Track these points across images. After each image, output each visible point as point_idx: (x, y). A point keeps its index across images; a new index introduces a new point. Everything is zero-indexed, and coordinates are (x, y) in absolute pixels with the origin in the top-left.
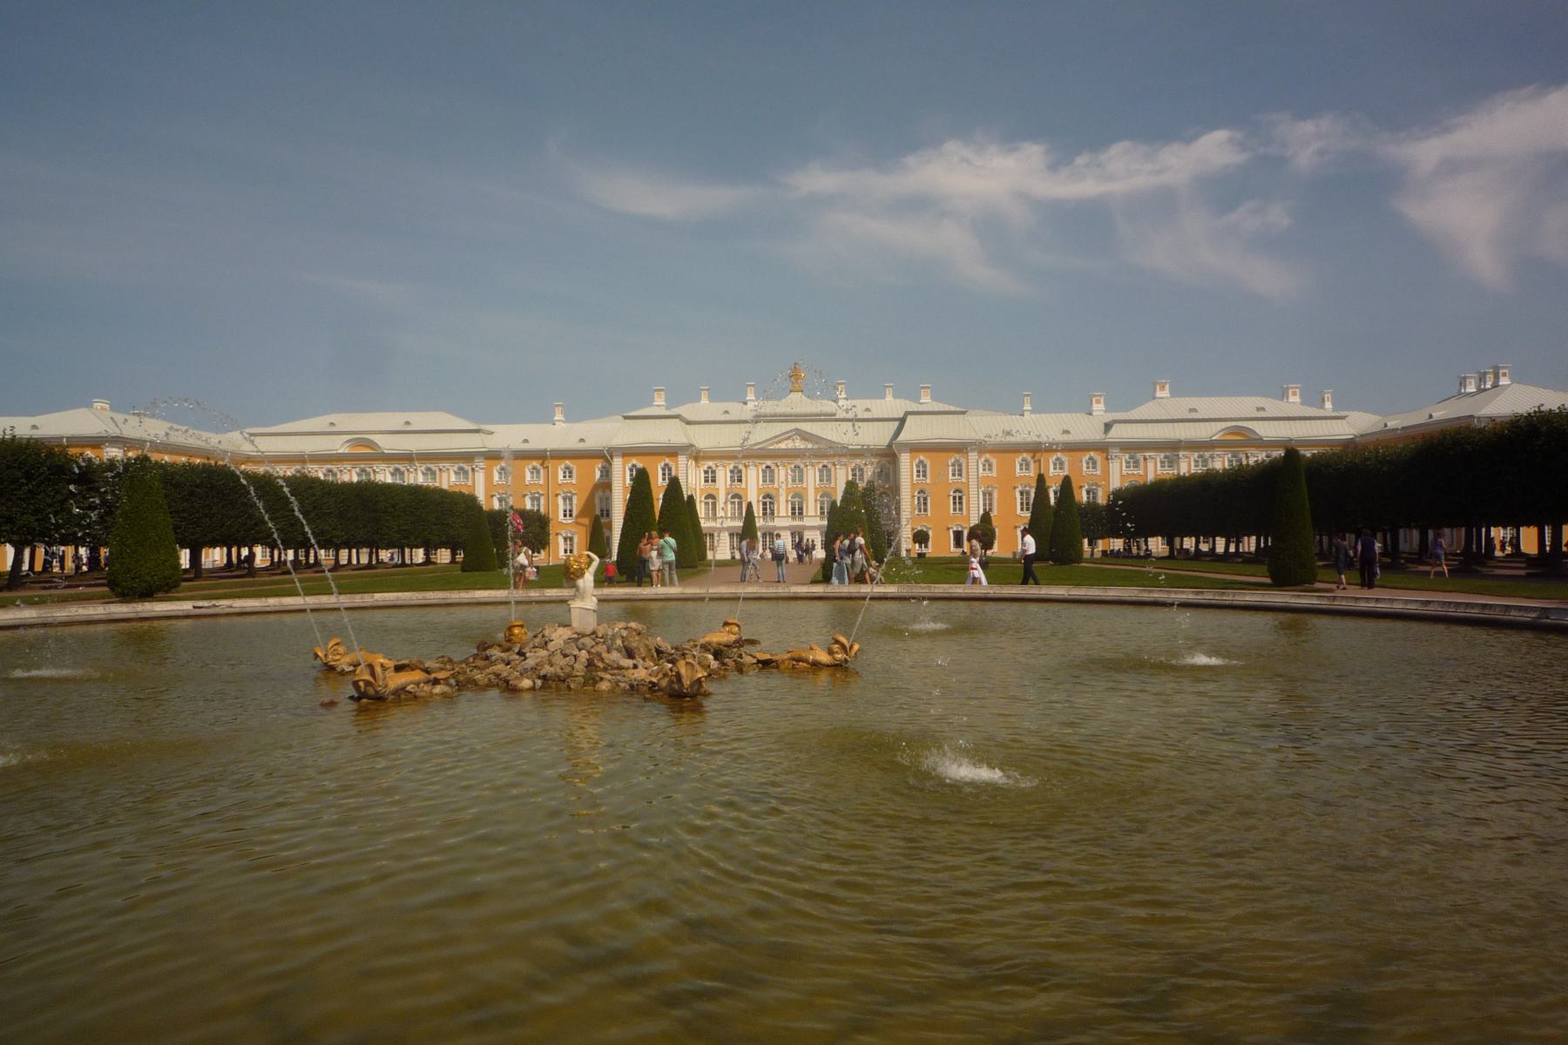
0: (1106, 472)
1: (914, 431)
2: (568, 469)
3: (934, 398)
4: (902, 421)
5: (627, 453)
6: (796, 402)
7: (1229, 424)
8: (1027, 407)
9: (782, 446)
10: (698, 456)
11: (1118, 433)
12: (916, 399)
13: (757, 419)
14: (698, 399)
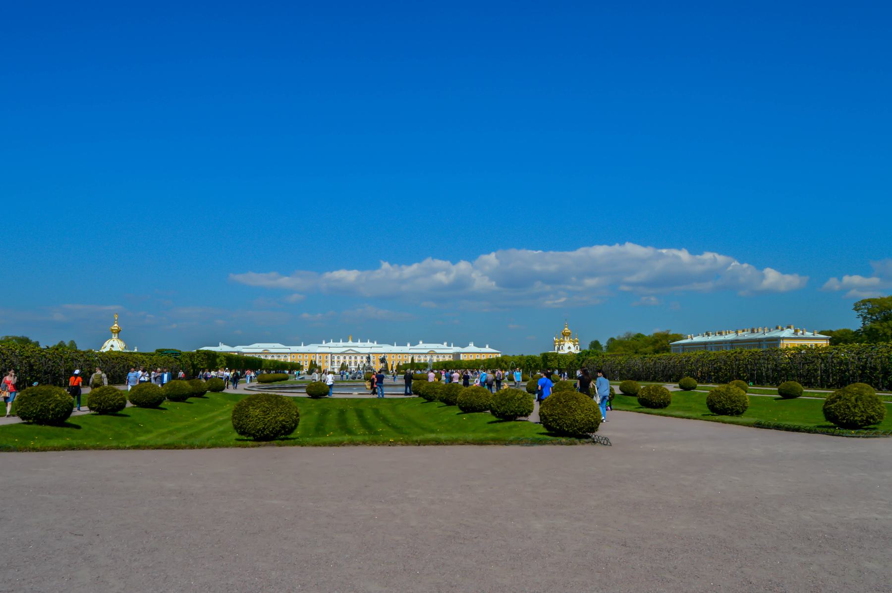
0: (408, 358)
1: (373, 350)
2: (294, 356)
3: (377, 343)
4: (371, 347)
5: (319, 353)
6: (350, 343)
7: (429, 350)
8: (395, 345)
9: (348, 352)
10: (332, 354)
11: (411, 351)
12: (374, 343)
13: (344, 347)
14: (330, 342)
